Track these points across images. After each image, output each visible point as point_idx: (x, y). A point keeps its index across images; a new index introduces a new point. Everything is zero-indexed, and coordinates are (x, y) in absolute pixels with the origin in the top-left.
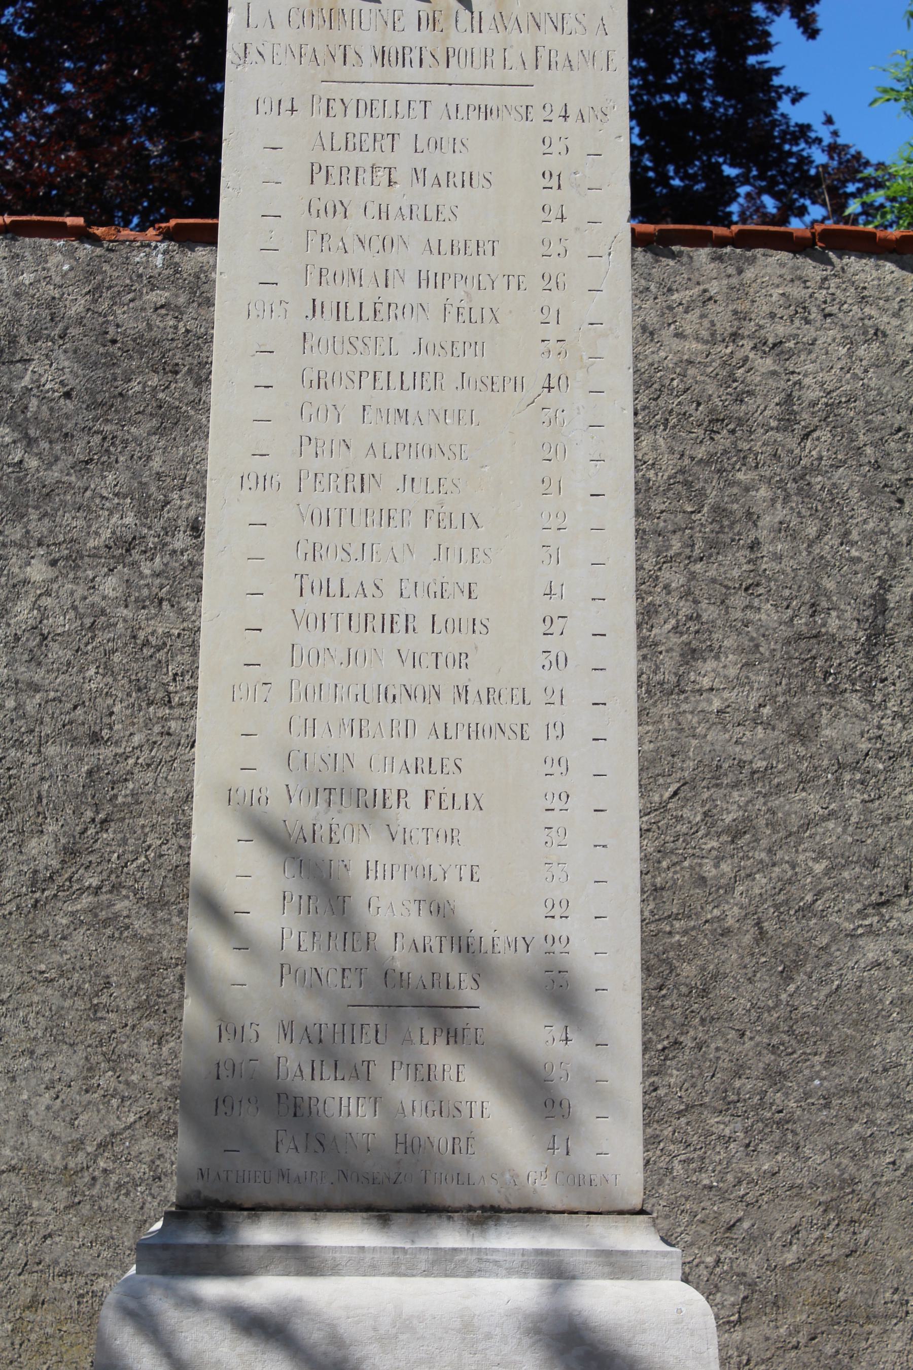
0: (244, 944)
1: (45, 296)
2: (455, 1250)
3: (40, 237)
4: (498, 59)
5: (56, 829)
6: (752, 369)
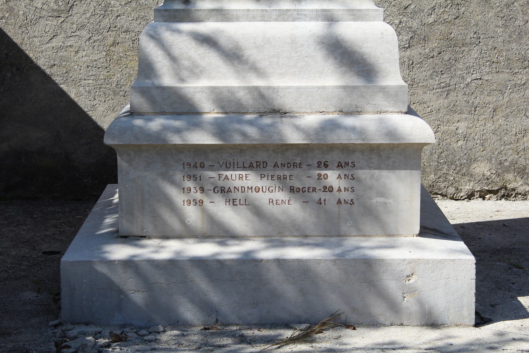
2: (288, 10)
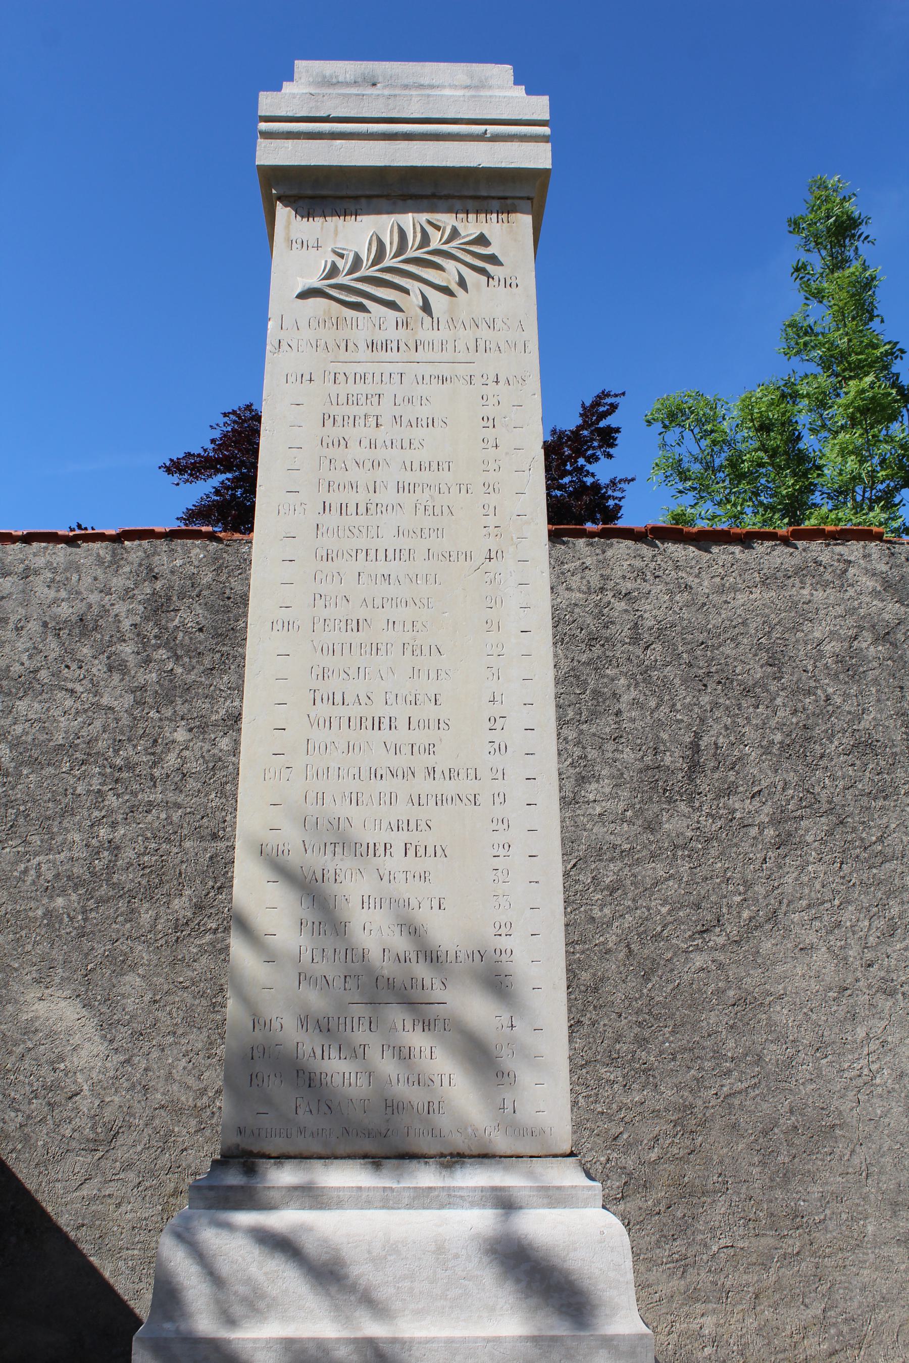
0: (270, 958)
2: (430, 1188)
4: (450, 347)
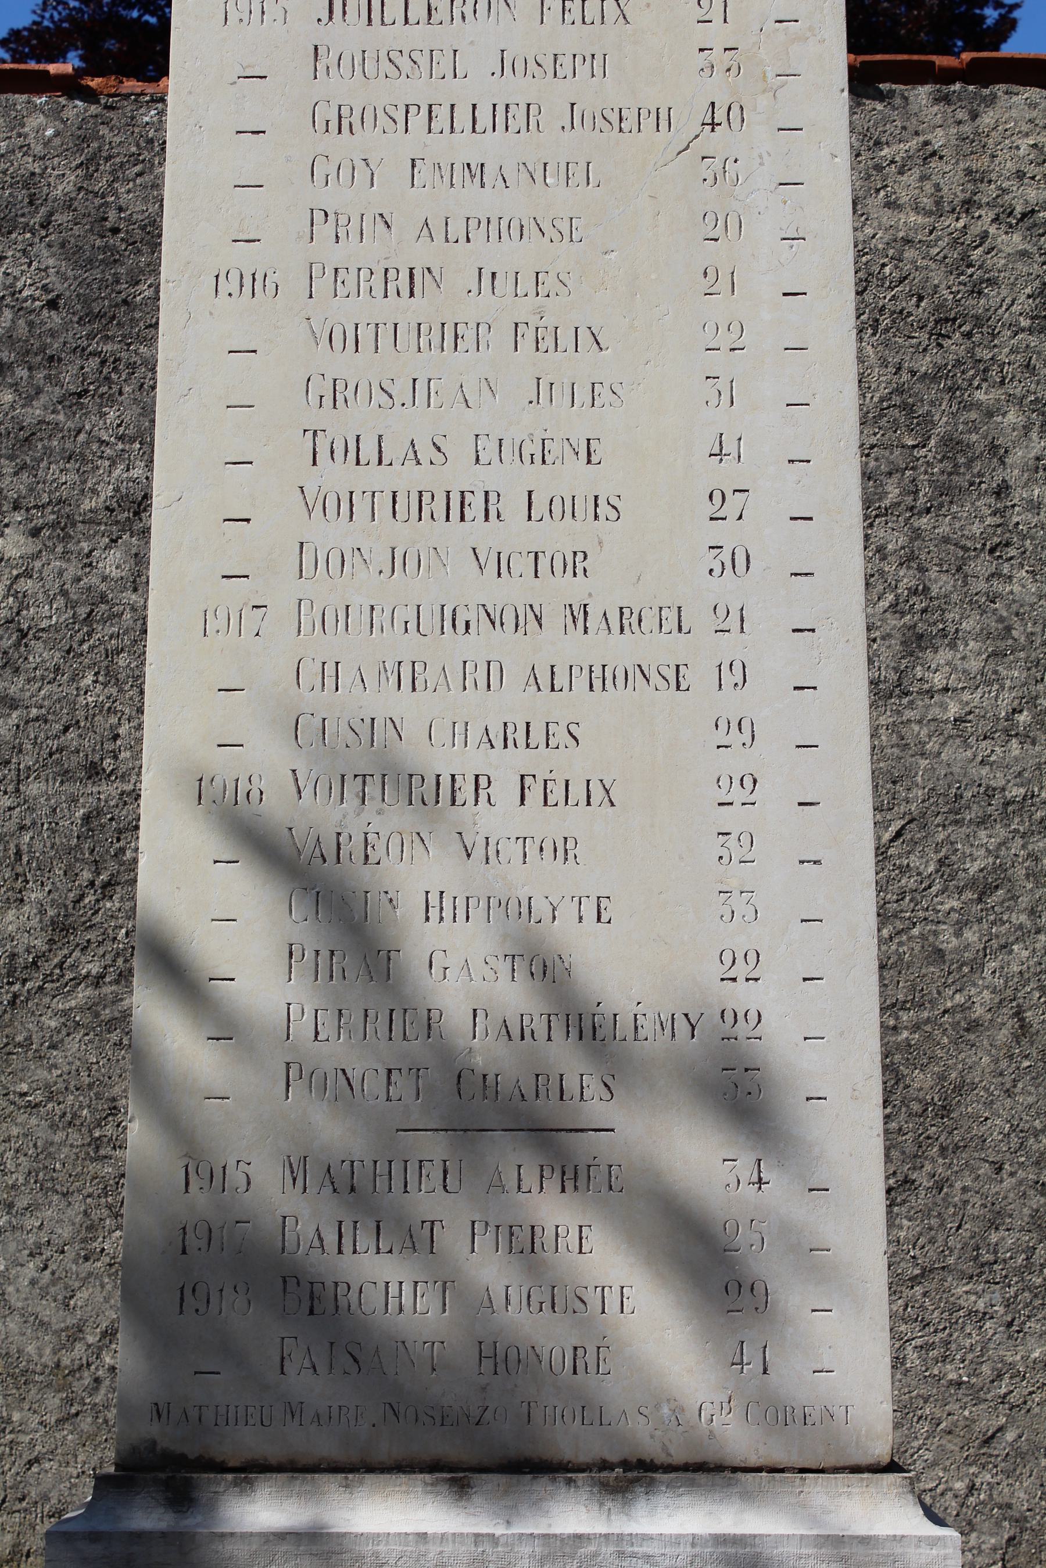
0: (226, 1029)
1: (22, 171)
2: (579, 1537)
3: (14, 93)
5: (40, 896)
6: (993, 249)
